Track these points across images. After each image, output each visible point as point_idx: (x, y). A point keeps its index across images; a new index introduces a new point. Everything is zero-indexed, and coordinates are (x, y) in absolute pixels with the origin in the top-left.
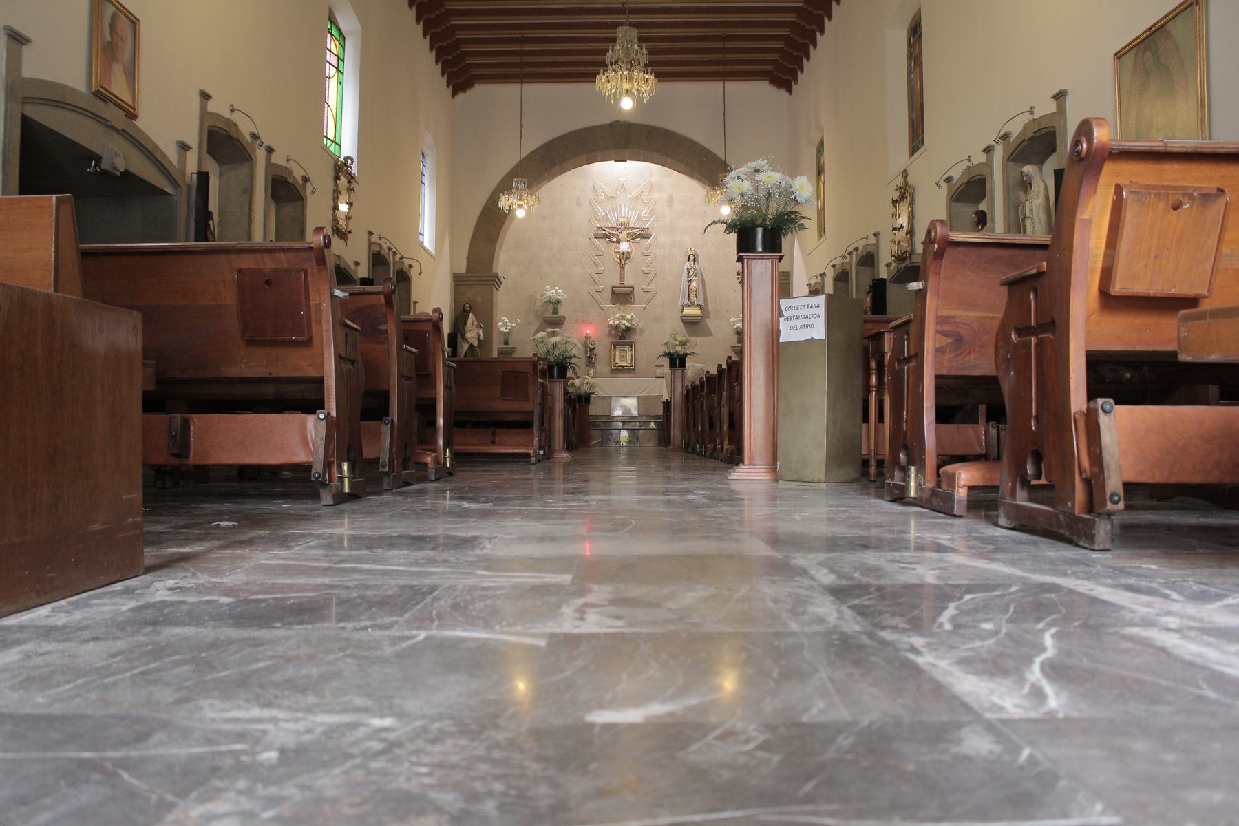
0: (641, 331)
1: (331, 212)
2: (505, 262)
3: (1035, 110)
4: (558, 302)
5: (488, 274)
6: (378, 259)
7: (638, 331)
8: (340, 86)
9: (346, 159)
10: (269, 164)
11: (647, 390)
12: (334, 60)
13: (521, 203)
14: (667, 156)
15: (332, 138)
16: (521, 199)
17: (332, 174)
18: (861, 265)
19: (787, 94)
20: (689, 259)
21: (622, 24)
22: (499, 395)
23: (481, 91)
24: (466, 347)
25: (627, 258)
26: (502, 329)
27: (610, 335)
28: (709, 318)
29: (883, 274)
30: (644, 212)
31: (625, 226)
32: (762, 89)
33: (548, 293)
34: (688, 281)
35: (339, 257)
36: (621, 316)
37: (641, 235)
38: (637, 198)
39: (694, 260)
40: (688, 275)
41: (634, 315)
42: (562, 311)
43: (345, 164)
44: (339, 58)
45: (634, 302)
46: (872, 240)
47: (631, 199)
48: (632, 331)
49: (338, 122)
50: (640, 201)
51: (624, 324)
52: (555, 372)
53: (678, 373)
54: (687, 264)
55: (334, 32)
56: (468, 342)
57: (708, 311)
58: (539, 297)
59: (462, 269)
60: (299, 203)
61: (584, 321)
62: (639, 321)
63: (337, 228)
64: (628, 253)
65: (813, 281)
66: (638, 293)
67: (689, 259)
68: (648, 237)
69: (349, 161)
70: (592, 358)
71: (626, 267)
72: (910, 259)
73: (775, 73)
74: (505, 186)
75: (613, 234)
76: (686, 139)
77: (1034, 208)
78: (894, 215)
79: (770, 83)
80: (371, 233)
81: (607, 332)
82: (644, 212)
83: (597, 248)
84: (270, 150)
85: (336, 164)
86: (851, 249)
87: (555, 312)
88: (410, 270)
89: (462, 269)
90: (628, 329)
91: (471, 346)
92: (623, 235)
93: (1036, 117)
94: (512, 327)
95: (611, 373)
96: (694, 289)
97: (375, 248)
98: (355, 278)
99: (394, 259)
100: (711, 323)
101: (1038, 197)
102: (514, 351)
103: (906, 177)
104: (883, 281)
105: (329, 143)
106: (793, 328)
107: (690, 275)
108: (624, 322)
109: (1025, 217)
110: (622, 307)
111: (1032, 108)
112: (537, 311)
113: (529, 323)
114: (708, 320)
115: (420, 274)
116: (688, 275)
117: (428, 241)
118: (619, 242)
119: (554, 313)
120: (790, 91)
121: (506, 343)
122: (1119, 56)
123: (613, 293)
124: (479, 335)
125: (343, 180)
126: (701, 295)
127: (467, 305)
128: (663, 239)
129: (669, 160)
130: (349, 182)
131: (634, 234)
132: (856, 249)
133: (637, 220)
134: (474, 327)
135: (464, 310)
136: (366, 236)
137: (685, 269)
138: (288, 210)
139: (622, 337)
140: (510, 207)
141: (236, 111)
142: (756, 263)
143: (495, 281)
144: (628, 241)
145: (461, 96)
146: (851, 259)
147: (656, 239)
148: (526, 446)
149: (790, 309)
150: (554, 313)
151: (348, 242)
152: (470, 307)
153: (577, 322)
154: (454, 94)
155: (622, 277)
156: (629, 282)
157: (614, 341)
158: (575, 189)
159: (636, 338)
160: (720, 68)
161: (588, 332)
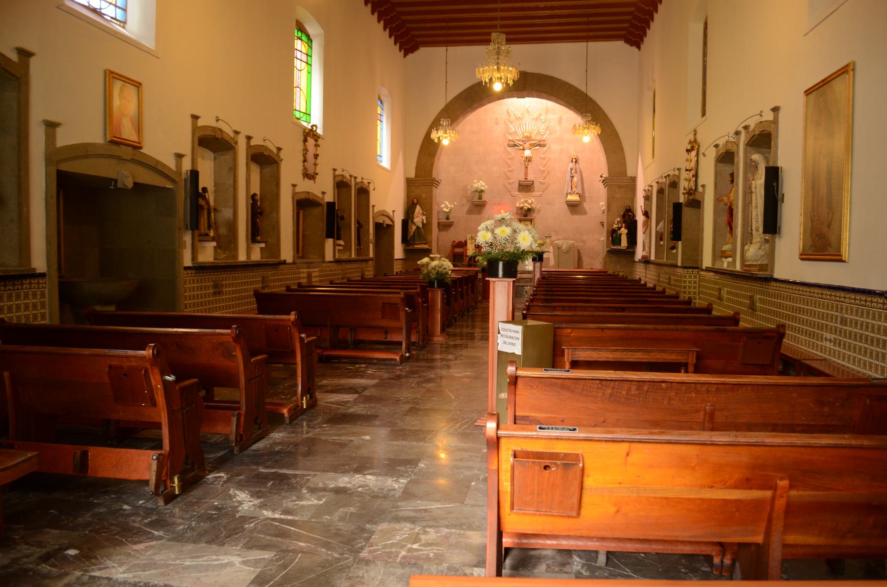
0: (539, 211)
1: (302, 163)
2: (443, 168)
3: (763, 114)
4: (482, 191)
5: (429, 179)
6: (341, 185)
7: (536, 211)
8: (309, 75)
9: (312, 126)
10: (249, 146)
12: (304, 58)
13: (446, 135)
14: (552, 95)
15: (304, 111)
16: (446, 133)
17: (302, 138)
18: (671, 187)
19: (637, 50)
20: (572, 161)
21: (495, 27)
22: (381, 316)
23: (423, 51)
24: (414, 228)
25: (529, 161)
26: (445, 210)
27: (517, 213)
28: (585, 202)
29: (682, 199)
30: (542, 127)
31: (528, 138)
32: (620, 46)
33: (475, 185)
35: (308, 192)
36: (525, 201)
37: (541, 144)
38: (537, 119)
39: (576, 162)
42: (485, 197)
43: (311, 130)
44: (307, 55)
46: (677, 173)
47: (533, 119)
49: (309, 99)
52: (436, 284)
53: (538, 264)
54: (571, 165)
55: (304, 38)
56: (415, 225)
57: (585, 198)
58: (469, 187)
59: (412, 175)
60: (275, 165)
61: (499, 204)
62: (537, 204)
63: (307, 174)
65: (647, 188)
66: (535, 184)
67: (572, 161)
68: (544, 146)
69: (315, 128)
71: (529, 167)
72: (695, 195)
73: (628, 36)
74: (435, 124)
75: (521, 145)
76: (566, 83)
77: (757, 186)
78: (687, 160)
79: (625, 42)
80: (335, 170)
81: (515, 212)
82: (542, 127)
83: (509, 154)
84: (249, 138)
85: (304, 132)
86: (666, 175)
87: (480, 198)
88: (368, 186)
89: (412, 175)
90: (529, 210)
91: (418, 227)
92: (527, 145)
93: (763, 119)
94: (451, 207)
96: (575, 183)
97: (339, 179)
98: (322, 203)
99: (355, 181)
100: (586, 205)
101: (761, 178)
103: (695, 134)
104: (682, 203)
105: (302, 114)
106: (505, 343)
108: (526, 205)
109: (751, 192)
110: (526, 194)
111: (761, 112)
112: (469, 197)
114: (584, 203)
115: (374, 190)
117: (385, 162)
118: (524, 149)
119: (479, 199)
120: (639, 48)
121: (448, 218)
122: (808, 92)
123: (520, 185)
124: (423, 220)
125: (311, 142)
126: (580, 186)
127: (415, 200)
128: (554, 147)
129: (554, 98)
130: (316, 141)
131: (534, 144)
132: (669, 175)
133: (537, 134)
134: (420, 215)
135: (413, 203)
136: (331, 172)
137: (569, 168)
138: (268, 170)
139: (525, 215)
140: (439, 138)
141: (220, 121)
142: (498, 284)
143: (433, 183)
144: (530, 149)
145: (410, 56)
146: (666, 180)
147: (549, 147)
148: (396, 353)
149: (504, 330)
150: (479, 199)
151: (316, 180)
152: (417, 201)
153: (494, 204)
154: (405, 55)
155: (526, 174)
156: (531, 177)
157: (519, 217)
159: (534, 216)
160: (584, 34)
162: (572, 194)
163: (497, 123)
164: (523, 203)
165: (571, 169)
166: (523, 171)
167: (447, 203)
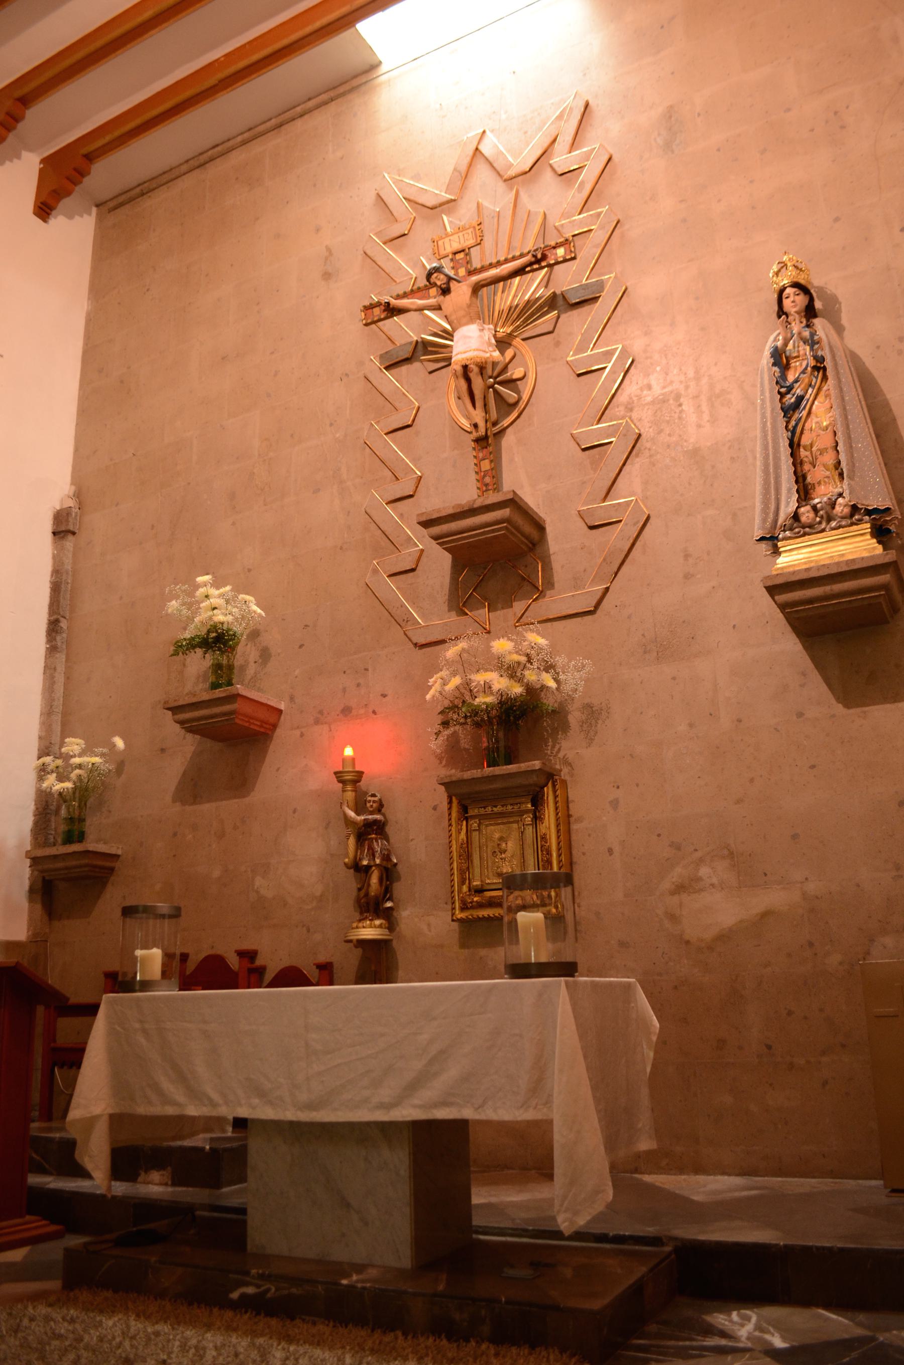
0: (593, 714)
7: (574, 718)
11: (452, 1072)
34: (789, 411)
39: (810, 312)
40: (784, 376)
41: (542, 641)
45: (549, 583)
48: (546, 723)
50: (548, 175)
51: (487, 688)
61: (346, 711)
64: (511, 383)
70: (368, 868)
81: (436, 745)
83: (389, 403)
95: (463, 945)
96: (826, 441)
102: (112, 870)
107: (791, 377)
110: (503, 617)
113: (163, 750)
116: (780, 381)
119: (215, 686)
121: (74, 835)
137: (766, 359)
150: (215, 686)
158: (318, 230)
161: (349, 752)
162: (809, 529)
163: (327, 276)
164: (464, 665)
165: (781, 360)
166: (473, 477)
167: (74, 745)
